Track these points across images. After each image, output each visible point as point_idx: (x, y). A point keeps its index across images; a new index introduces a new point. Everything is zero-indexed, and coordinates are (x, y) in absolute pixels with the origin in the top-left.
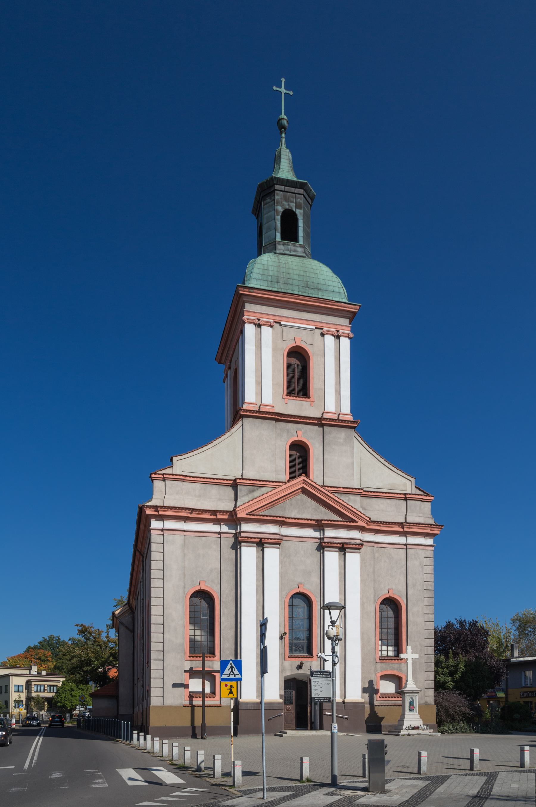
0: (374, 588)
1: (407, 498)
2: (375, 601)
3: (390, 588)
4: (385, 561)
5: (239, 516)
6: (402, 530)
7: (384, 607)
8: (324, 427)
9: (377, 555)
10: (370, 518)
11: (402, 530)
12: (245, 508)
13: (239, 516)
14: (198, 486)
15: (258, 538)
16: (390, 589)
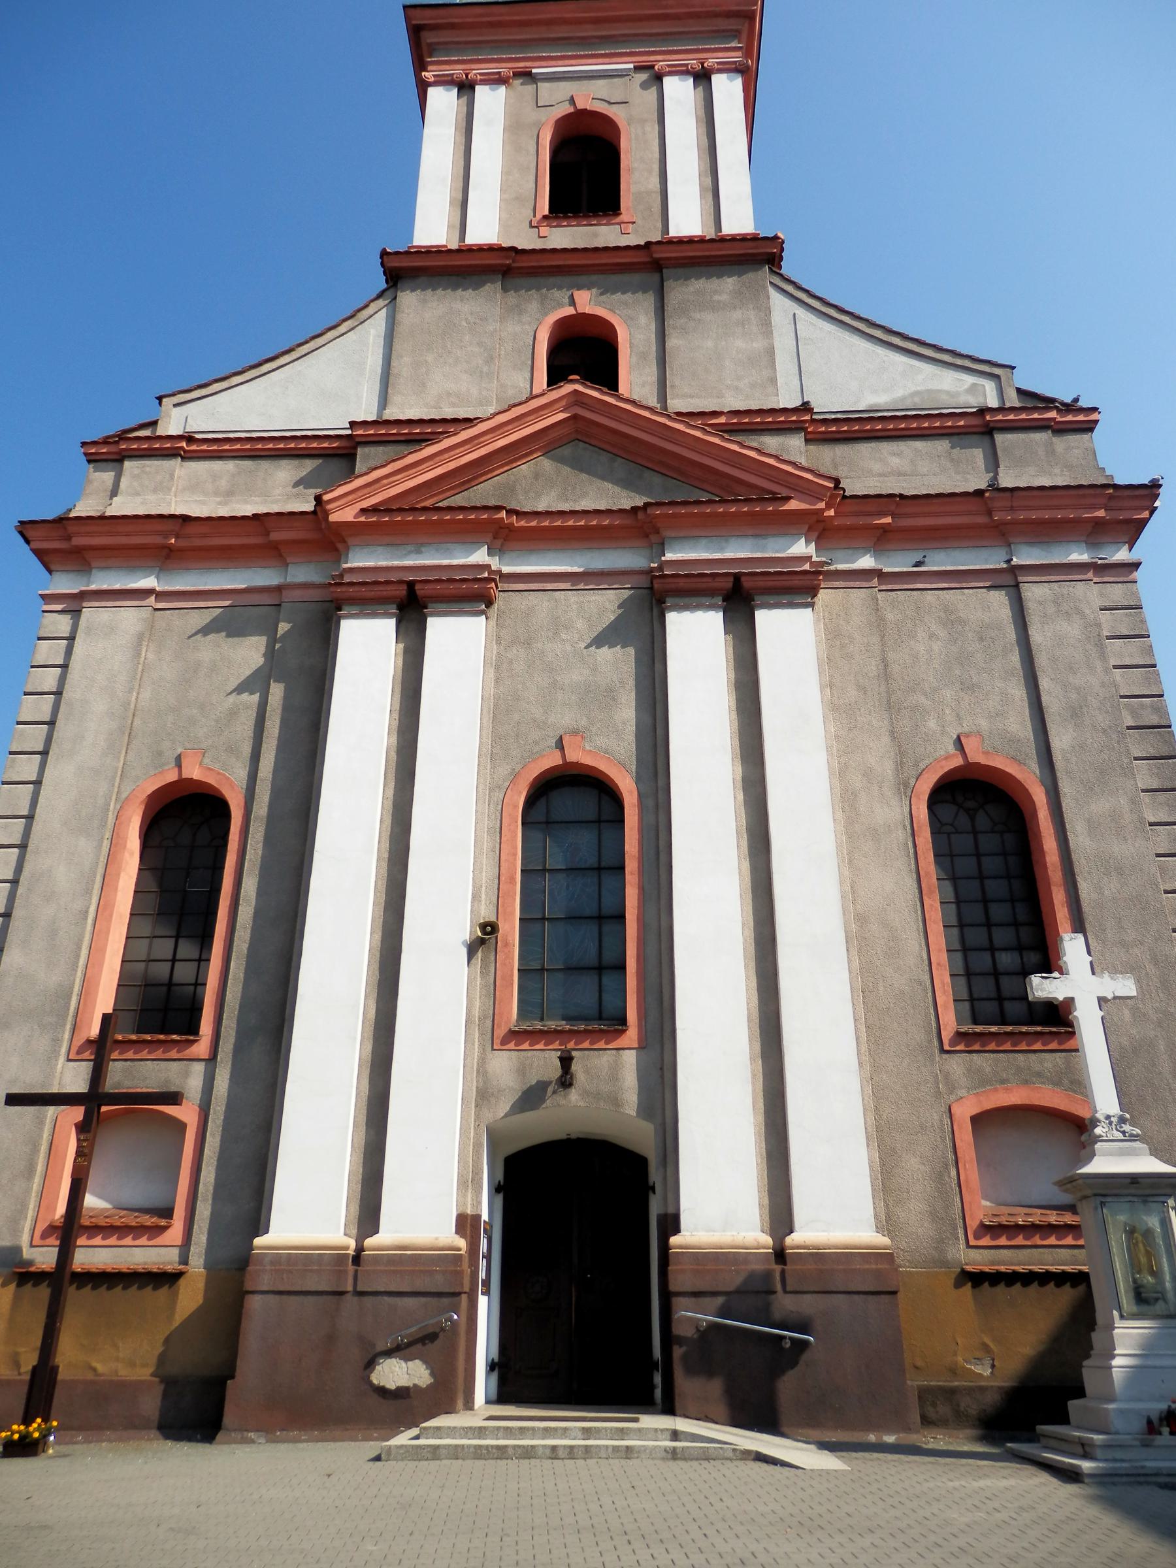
0: (892, 733)
1: (992, 425)
2: (906, 785)
3: (966, 730)
4: (932, 636)
5: (333, 518)
6: (982, 519)
7: (947, 812)
8: (665, 271)
9: (890, 616)
10: (837, 482)
11: (982, 519)
12: (360, 493)
13: (333, 518)
14: (230, 466)
15: (401, 582)
16: (968, 736)
